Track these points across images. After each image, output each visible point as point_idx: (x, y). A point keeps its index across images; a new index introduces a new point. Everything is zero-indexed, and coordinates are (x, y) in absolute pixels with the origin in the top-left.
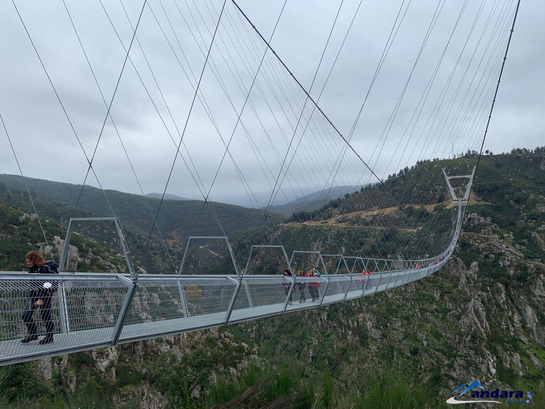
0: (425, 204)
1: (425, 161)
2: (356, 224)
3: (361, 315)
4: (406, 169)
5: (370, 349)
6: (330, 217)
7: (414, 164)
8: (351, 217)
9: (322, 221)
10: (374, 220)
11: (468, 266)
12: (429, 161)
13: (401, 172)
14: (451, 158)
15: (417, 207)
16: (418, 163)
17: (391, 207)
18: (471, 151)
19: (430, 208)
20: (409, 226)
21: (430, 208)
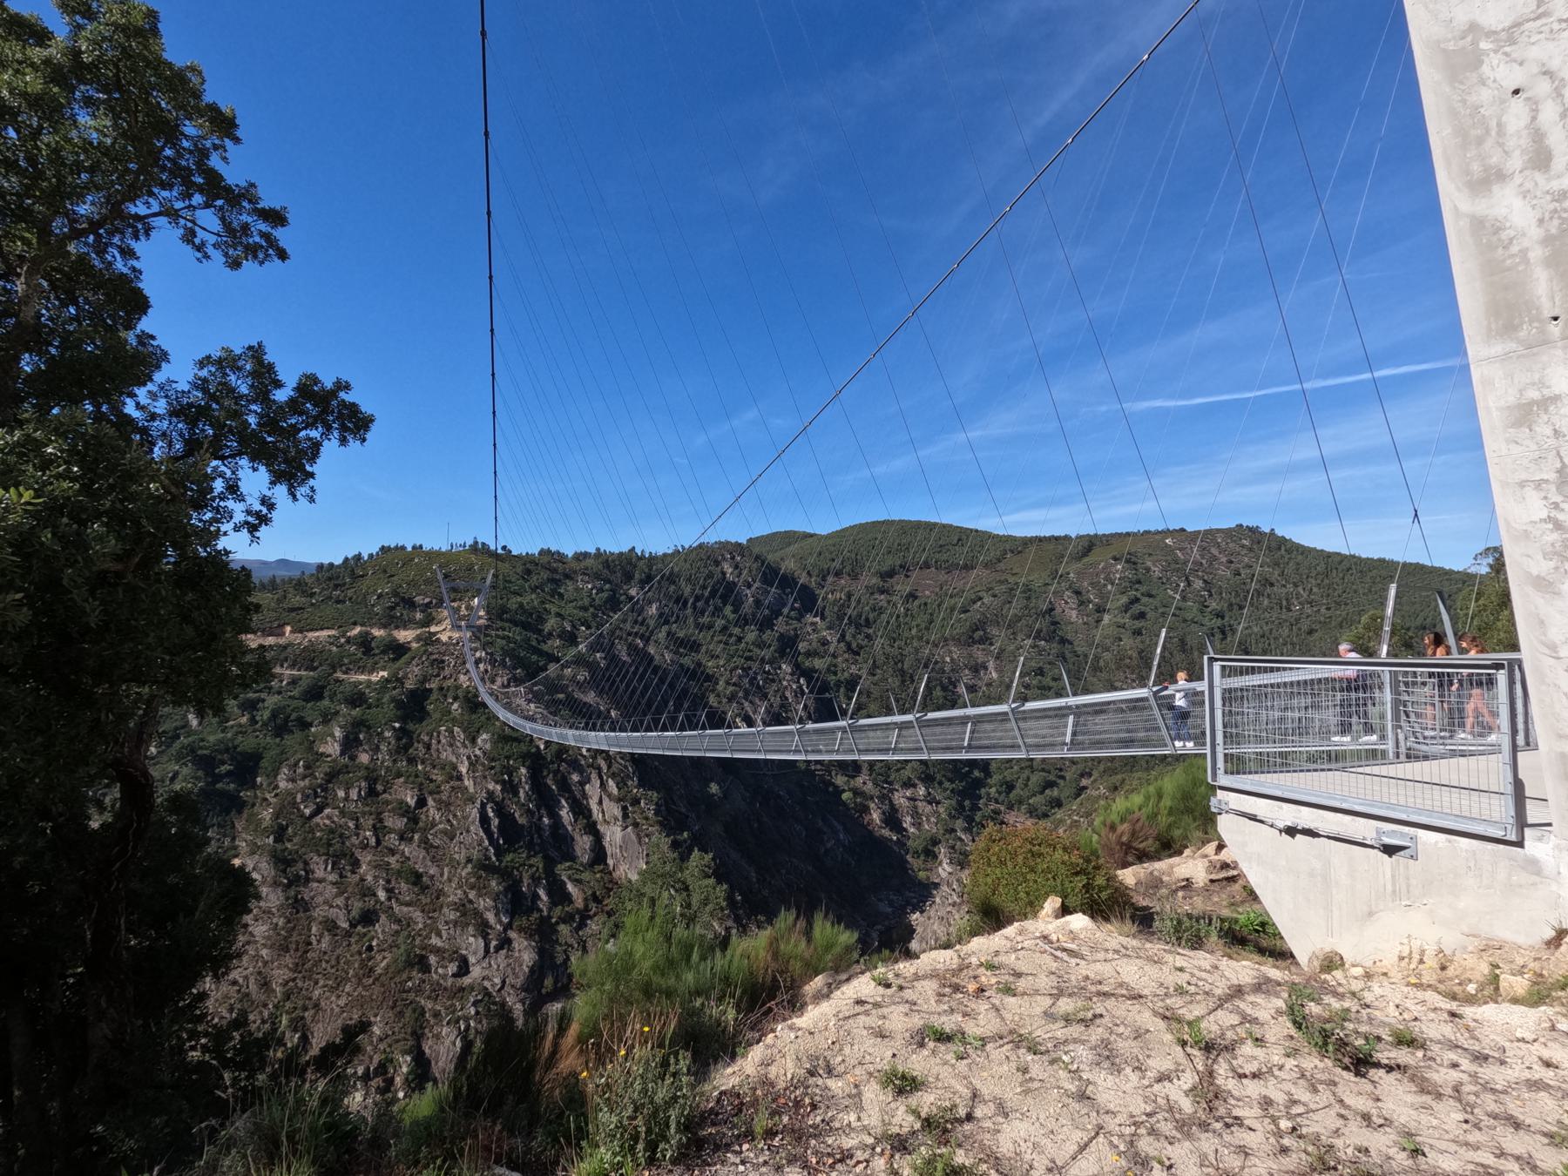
0: (397, 627)
1: (397, 548)
4: (358, 557)
5: (251, 934)
7: (375, 550)
11: (473, 741)
12: (403, 548)
13: (346, 559)
14: (443, 550)
15: (378, 633)
18: (480, 541)
20: (362, 669)
21: (405, 635)
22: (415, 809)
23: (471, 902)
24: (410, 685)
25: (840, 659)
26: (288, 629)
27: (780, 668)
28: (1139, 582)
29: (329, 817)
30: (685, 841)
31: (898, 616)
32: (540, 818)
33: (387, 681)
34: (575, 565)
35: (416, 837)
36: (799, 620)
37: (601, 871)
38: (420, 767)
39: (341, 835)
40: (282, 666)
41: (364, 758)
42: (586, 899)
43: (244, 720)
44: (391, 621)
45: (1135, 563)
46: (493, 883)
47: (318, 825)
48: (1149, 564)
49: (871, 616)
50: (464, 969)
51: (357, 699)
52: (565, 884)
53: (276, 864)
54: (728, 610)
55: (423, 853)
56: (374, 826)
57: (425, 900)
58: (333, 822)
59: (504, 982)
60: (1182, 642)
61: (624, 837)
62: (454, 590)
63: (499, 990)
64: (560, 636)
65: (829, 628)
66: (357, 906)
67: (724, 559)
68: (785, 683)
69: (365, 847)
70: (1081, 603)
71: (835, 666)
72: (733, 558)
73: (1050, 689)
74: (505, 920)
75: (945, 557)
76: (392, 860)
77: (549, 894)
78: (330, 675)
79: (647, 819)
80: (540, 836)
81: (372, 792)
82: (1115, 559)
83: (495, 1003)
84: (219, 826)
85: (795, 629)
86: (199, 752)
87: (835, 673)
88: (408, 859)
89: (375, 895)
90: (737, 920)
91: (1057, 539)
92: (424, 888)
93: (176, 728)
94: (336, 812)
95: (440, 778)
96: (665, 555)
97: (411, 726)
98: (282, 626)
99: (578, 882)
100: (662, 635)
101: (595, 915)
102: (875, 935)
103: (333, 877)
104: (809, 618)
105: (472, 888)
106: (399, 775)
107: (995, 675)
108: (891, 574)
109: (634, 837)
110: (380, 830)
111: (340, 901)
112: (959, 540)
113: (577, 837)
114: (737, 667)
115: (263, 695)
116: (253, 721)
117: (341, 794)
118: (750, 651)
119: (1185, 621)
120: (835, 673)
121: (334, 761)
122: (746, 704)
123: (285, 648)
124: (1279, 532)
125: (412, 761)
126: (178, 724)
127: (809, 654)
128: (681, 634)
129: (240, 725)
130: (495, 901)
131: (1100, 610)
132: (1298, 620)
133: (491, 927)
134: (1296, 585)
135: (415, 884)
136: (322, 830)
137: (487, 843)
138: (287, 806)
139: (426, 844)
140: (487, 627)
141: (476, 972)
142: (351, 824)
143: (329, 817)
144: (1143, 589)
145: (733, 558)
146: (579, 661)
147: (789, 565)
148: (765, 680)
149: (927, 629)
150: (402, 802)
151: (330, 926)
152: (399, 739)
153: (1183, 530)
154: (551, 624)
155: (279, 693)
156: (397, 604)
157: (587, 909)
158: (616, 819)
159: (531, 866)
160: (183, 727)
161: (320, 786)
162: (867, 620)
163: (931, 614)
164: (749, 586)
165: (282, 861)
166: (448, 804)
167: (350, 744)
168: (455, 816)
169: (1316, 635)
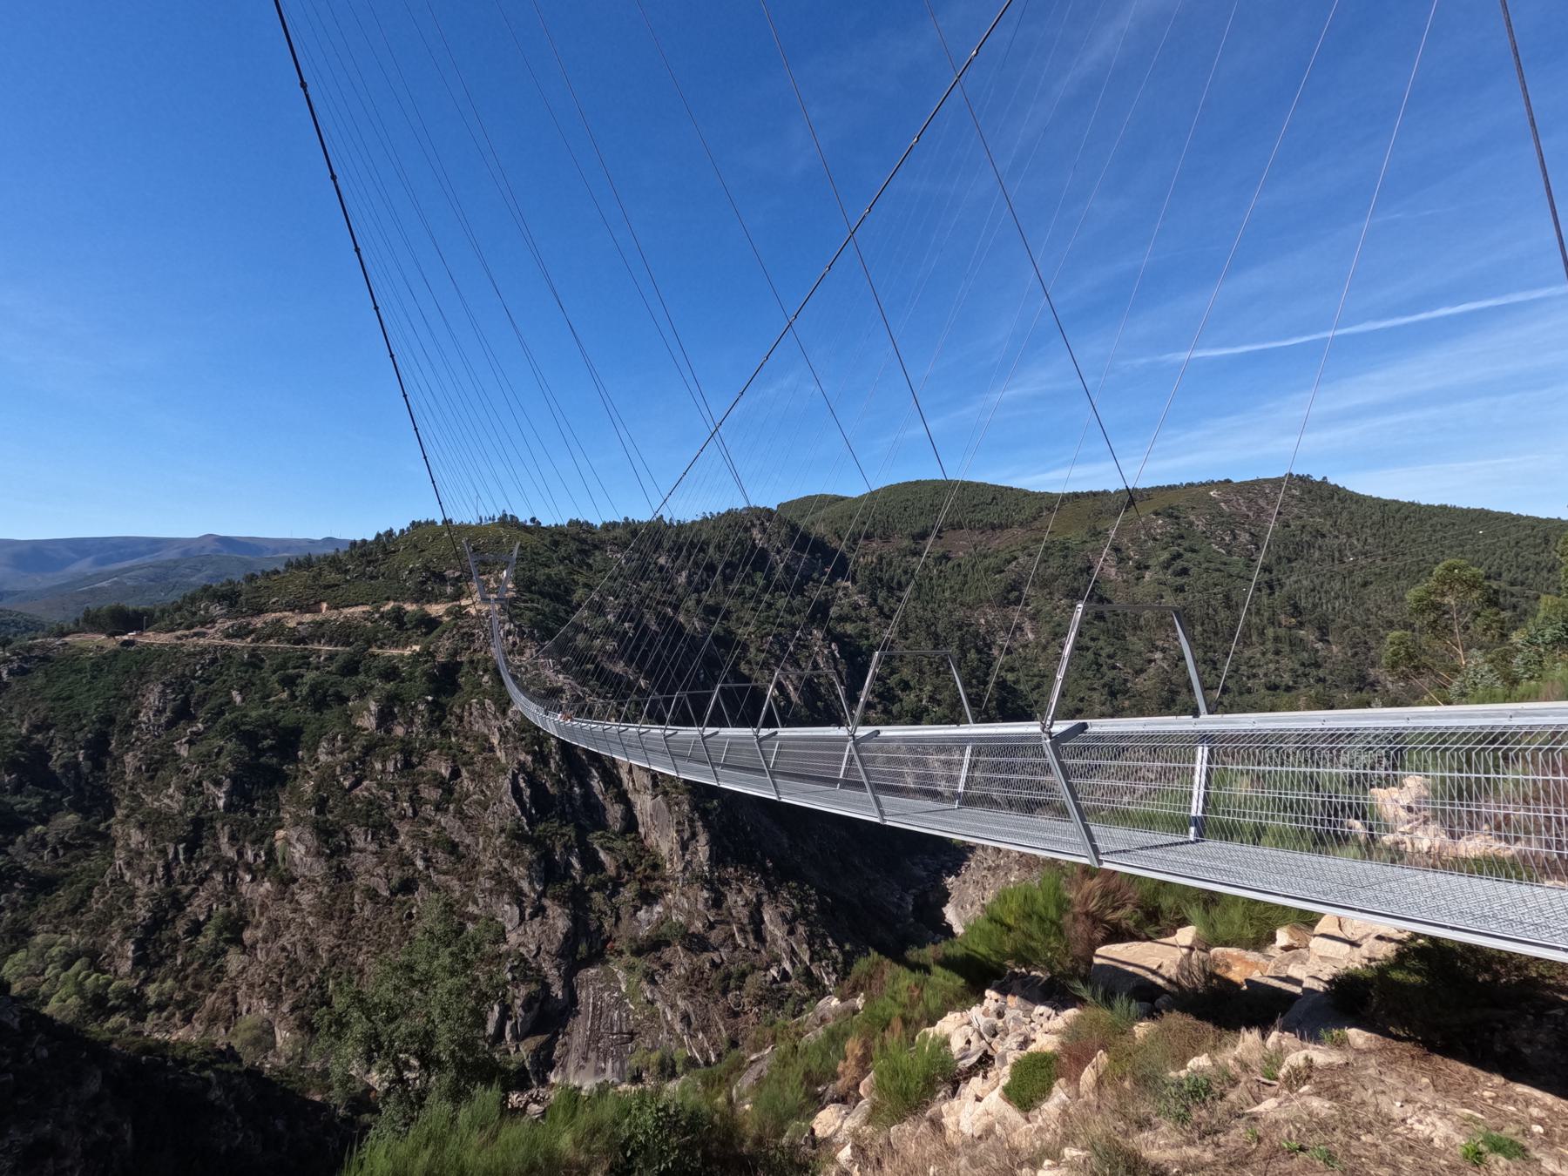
0: (429, 602)
1: (427, 523)
3: (280, 833)
4: (390, 533)
5: (298, 902)
7: (406, 525)
8: (259, 625)
9: (179, 633)
10: (319, 631)
12: (433, 523)
13: (379, 535)
15: (410, 607)
16: (413, 523)
17: (357, 605)
19: (436, 610)
21: (436, 610)
22: (450, 779)
23: (505, 870)
24: (441, 658)
25: (872, 624)
26: (324, 605)
27: (811, 634)
28: (1182, 537)
29: (367, 789)
30: (715, 809)
31: (931, 579)
32: (571, 787)
33: (419, 654)
34: (604, 536)
35: (452, 807)
37: (633, 839)
38: (453, 739)
39: (380, 807)
40: (319, 642)
41: (399, 731)
42: (618, 867)
43: (285, 695)
44: (423, 596)
45: (1177, 518)
46: (527, 852)
47: (357, 797)
48: (1192, 518)
49: (903, 579)
50: (501, 936)
51: (390, 673)
52: (598, 852)
53: (318, 834)
55: (459, 823)
56: (410, 797)
57: (461, 869)
58: (372, 794)
59: (539, 948)
60: (1227, 597)
61: (654, 806)
62: (484, 563)
63: (535, 957)
64: (589, 607)
65: (861, 592)
66: (397, 875)
67: (753, 525)
69: (403, 817)
70: (1121, 560)
71: (867, 630)
73: (1088, 649)
74: (539, 888)
75: (979, 516)
76: (429, 830)
77: (582, 862)
78: (366, 650)
79: (676, 787)
80: (572, 806)
81: (408, 765)
82: (1156, 514)
83: (531, 969)
84: (265, 799)
85: (826, 594)
86: (242, 728)
87: (867, 638)
88: (445, 829)
89: (413, 864)
90: (769, 887)
91: (1095, 494)
92: (460, 858)
93: (221, 705)
94: (374, 784)
95: (473, 750)
96: (694, 522)
97: (443, 700)
98: (318, 603)
99: (609, 850)
100: (691, 603)
101: (628, 882)
102: (910, 899)
103: (373, 847)
105: (506, 857)
106: (433, 747)
107: (1031, 636)
109: (664, 806)
110: (416, 800)
111: (380, 870)
112: (994, 498)
113: (608, 806)
115: (302, 671)
116: (293, 696)
117: (378, 766)
119: (1230, 576)
120: (867, 638)
121: (371, 734)
123: (322, 624)
124: (1332, 481)
125: (445, 733)
126: (223, 700)
127: (842, 619)
129: (281, 701)
130: (528, 869)
131: (1142, 567)
132: (1351, 573)
133: (525, 895)
134: (1349, 536)
135: (451, 853)
136: (361, 802)
137: (519, 813)
138: (327, 779)
139: (460, 814)
140: (515, 599)
141: (513, 938)
142: (389, 796)
143: (367, 789)
144: (1186, 544)
145: (762, 524)
146: (608, 631)
147: (820, 530)
149: (961, 591)
150: (436, 774)
151: (372, 894)
152: (431, 712)
153: (1228, 481)
154: (579, 594)
155: (317, 668)
156: (428, 579)
157: (619, 876)
158: (646, 788)
159: (563, 835)
160: (228, 703)
161: (358, 759)
162: (899, 583)
163: (965, 576)
164: (779, 552)
165: (324, 832)
166: (481, 775)
167: (385, 718)
168: (488, 786)
169: (1371, 588)
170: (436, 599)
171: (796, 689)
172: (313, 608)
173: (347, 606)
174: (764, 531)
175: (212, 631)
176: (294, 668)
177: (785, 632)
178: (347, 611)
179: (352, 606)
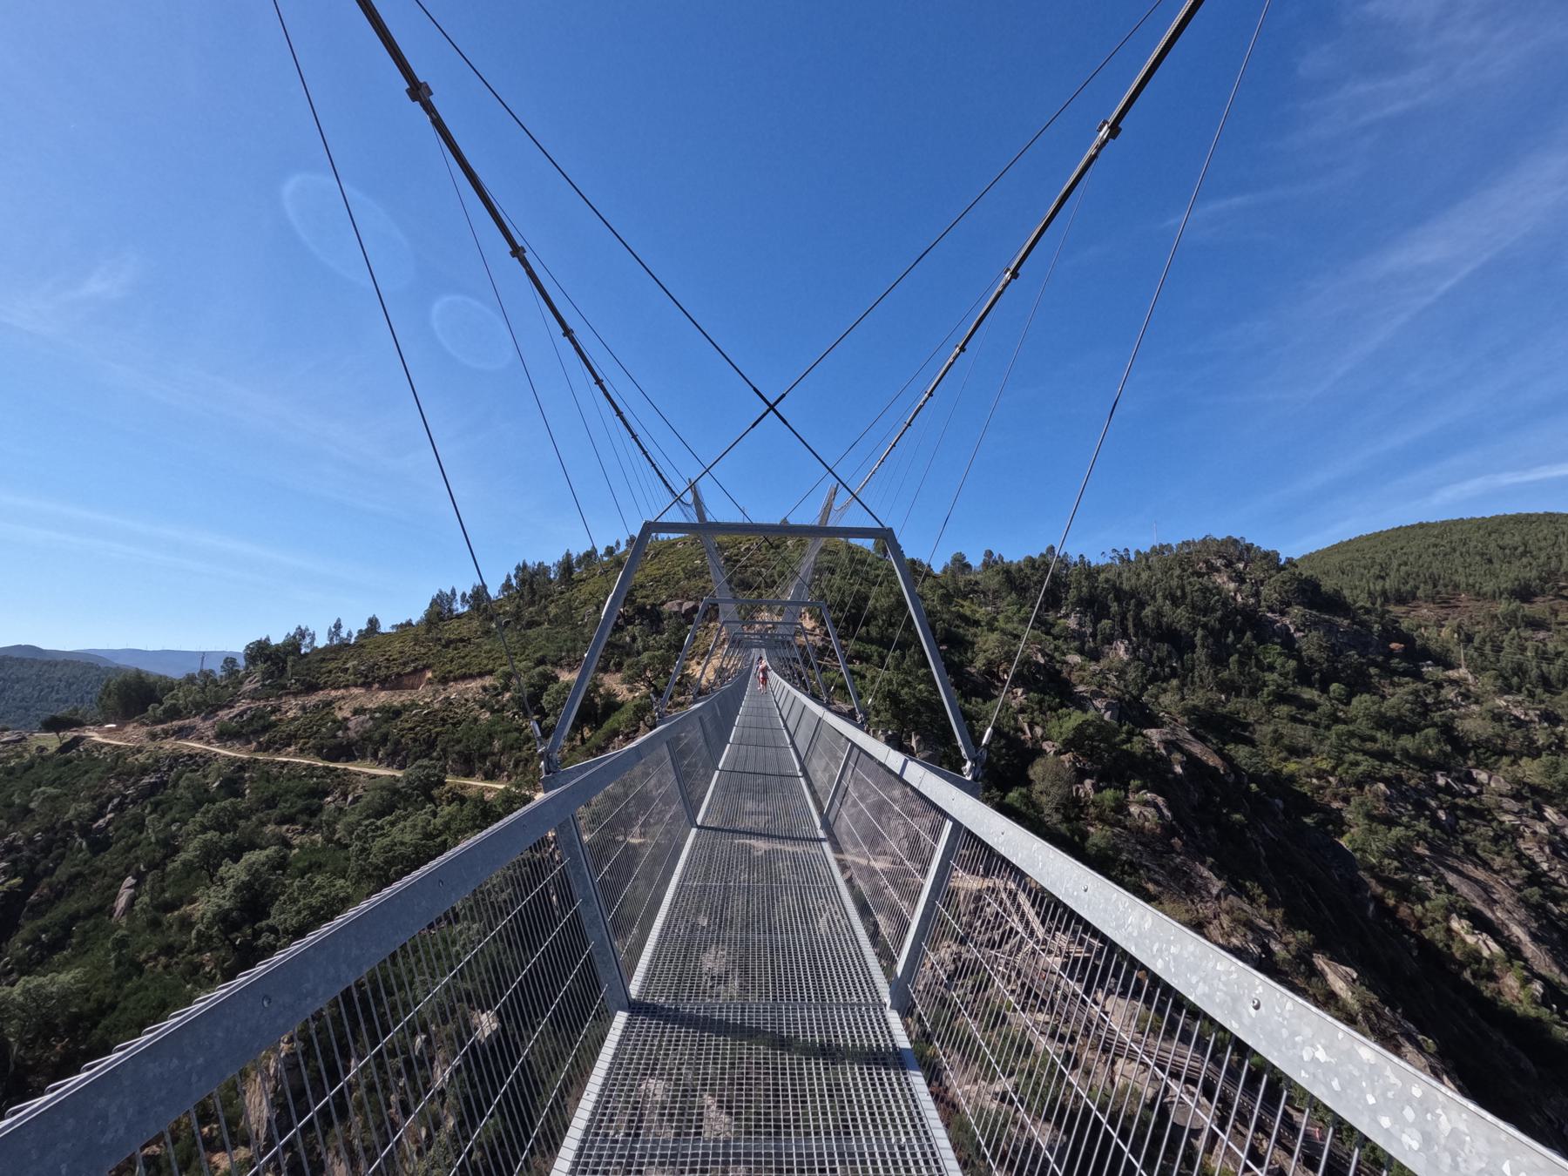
2: (293, 748)
6: (209, 708)
8: (291, 714)
17: (481, 675)
27: (1474, 781)
36: (1418, 676)
54: (1273, 653)
64: (1018, 680)
67: (1212, 569)
68: (1507, 818)
72: (1229, 564)
93: (75, 918)
104: (1428, 669)
108: (1524, 593)
114: (1371, 777)
118: (1374, 739)
122: (1452, 879)
123: (397, 713)
126: (94, 901)
128: (1197, 699)
148: (1452, 809)
164: (1283, 613)
170: (616, 655)
171: (1535, 938)
172: (406, 681)
173: (464, 677)
174: (1240, 578)
175: (209, 723)
176: (280, 823)
177: (1415, 779)
178: (454, 691)
179: (472, 677)
